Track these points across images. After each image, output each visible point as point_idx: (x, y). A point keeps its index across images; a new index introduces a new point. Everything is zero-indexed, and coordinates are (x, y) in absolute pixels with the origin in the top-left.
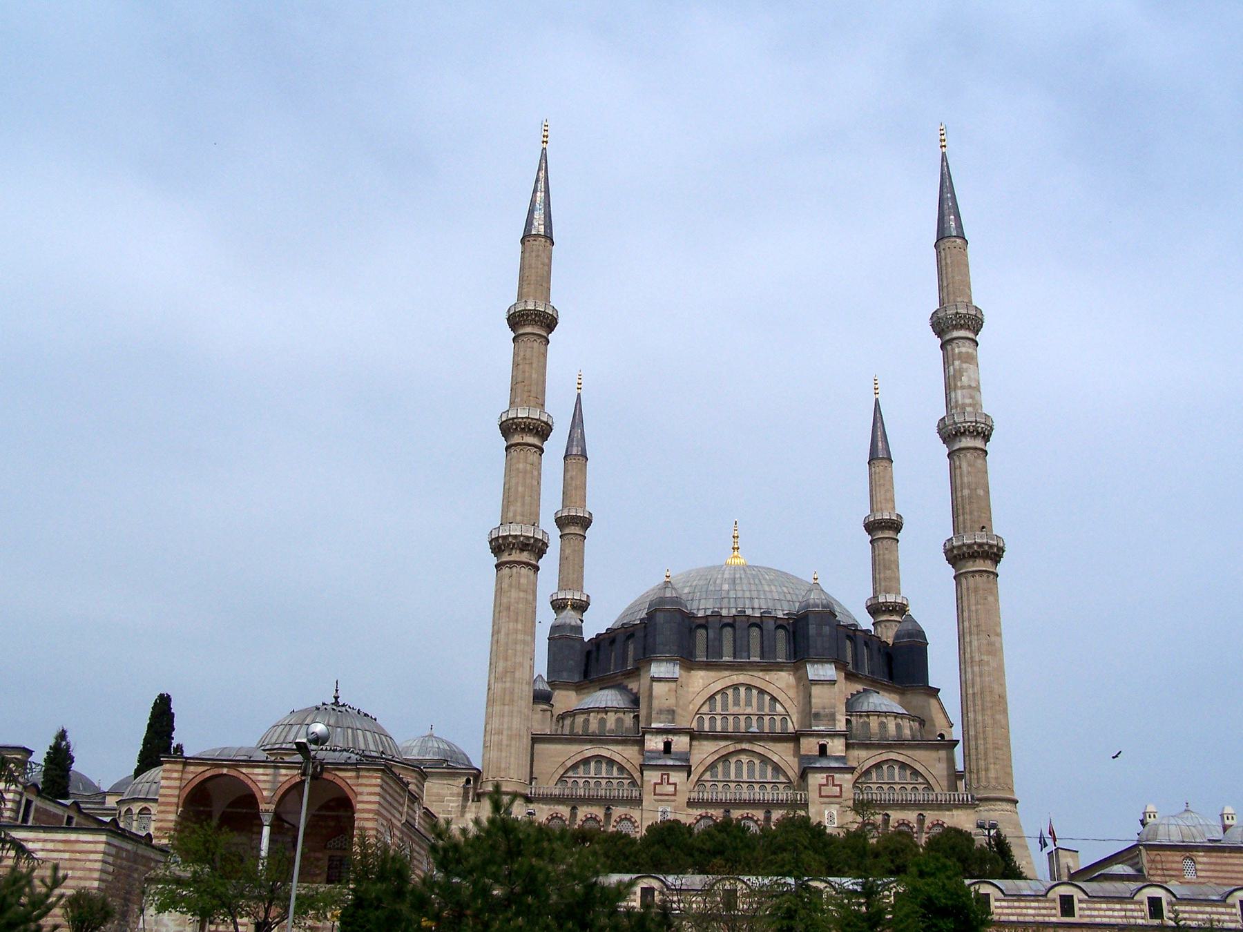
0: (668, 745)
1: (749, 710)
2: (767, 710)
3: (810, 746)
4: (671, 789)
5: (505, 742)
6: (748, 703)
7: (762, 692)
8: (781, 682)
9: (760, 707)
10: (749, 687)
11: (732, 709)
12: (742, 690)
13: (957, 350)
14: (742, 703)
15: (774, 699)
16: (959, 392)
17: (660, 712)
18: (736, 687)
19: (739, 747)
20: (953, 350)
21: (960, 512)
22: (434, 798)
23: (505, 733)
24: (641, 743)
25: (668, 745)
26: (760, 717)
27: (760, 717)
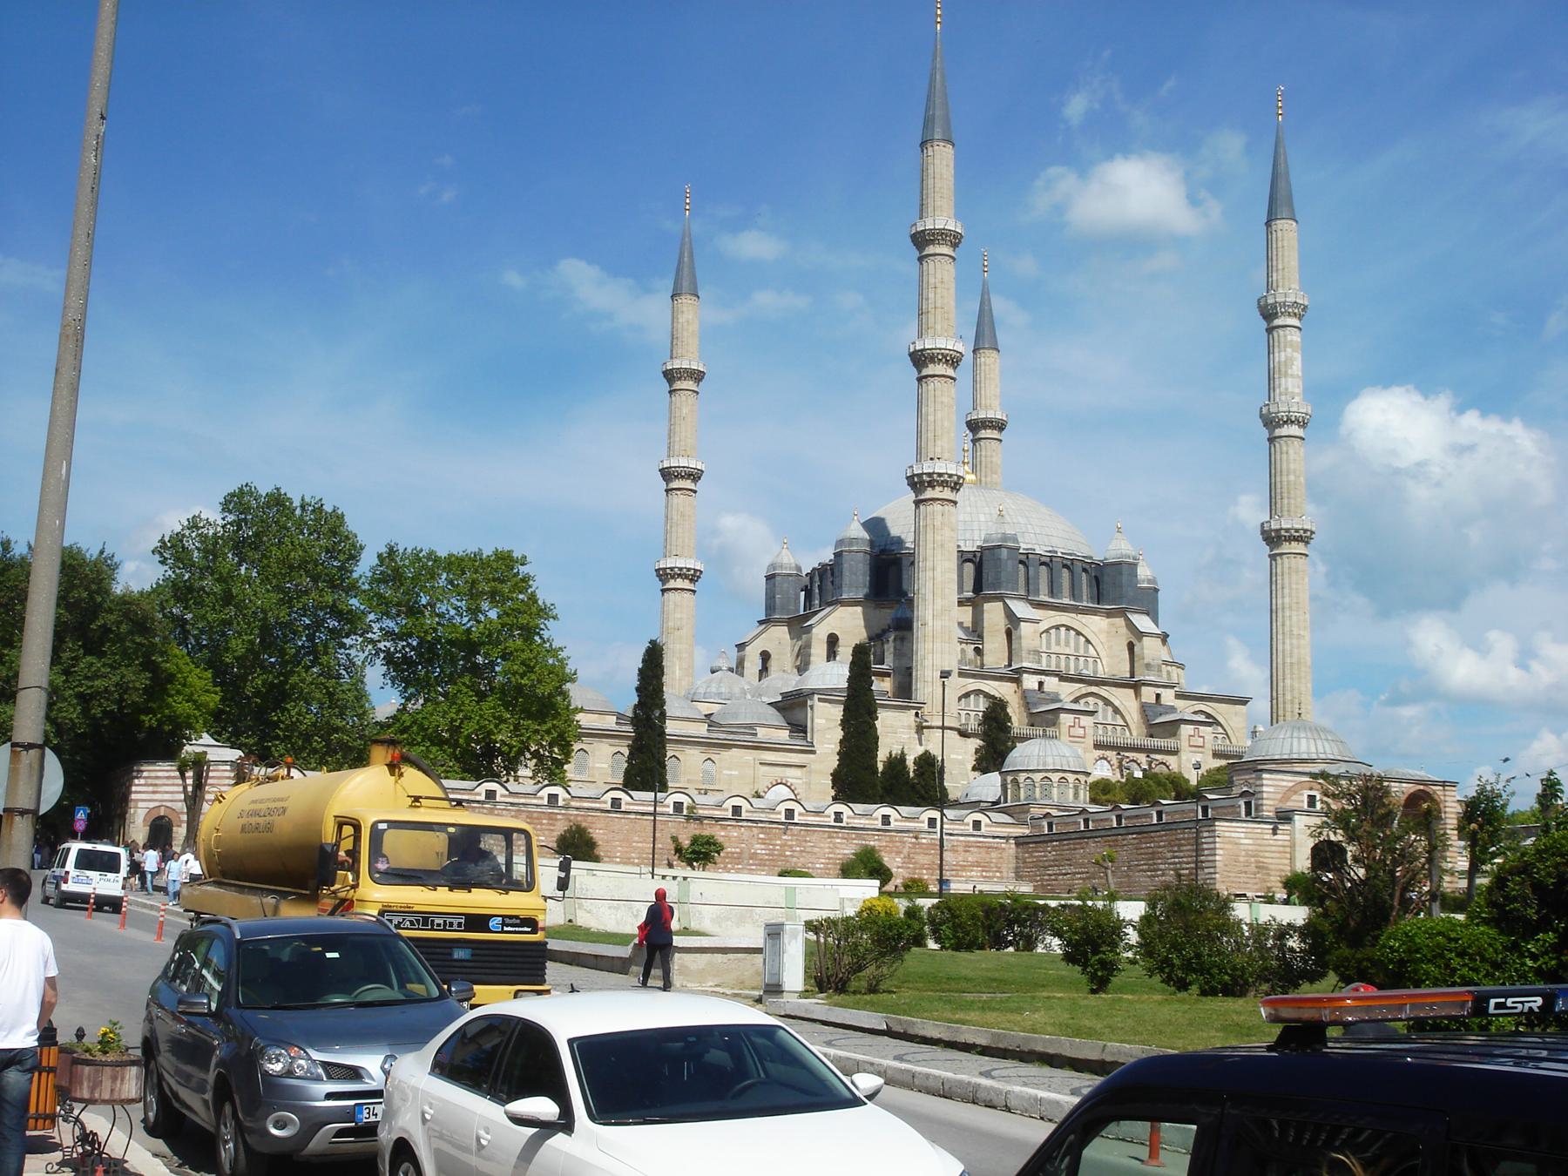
0: (1041, 684)
2: (1082, 652)
3: (1148, 694)
4: (1081, 731)
6: (1067, 644)
7: (1079, 633)
8: (1095, 625)
9: (1077, 649)
10: (1068, 628)
11: (1055, 649)
15: (1088, 641)
17: (1029, 652)
18: (1057, 627)
19: (1094, 689)
24: (1018, 681)
25: (1041, 684)
26: (1077, 658)
27: (1077, 658)
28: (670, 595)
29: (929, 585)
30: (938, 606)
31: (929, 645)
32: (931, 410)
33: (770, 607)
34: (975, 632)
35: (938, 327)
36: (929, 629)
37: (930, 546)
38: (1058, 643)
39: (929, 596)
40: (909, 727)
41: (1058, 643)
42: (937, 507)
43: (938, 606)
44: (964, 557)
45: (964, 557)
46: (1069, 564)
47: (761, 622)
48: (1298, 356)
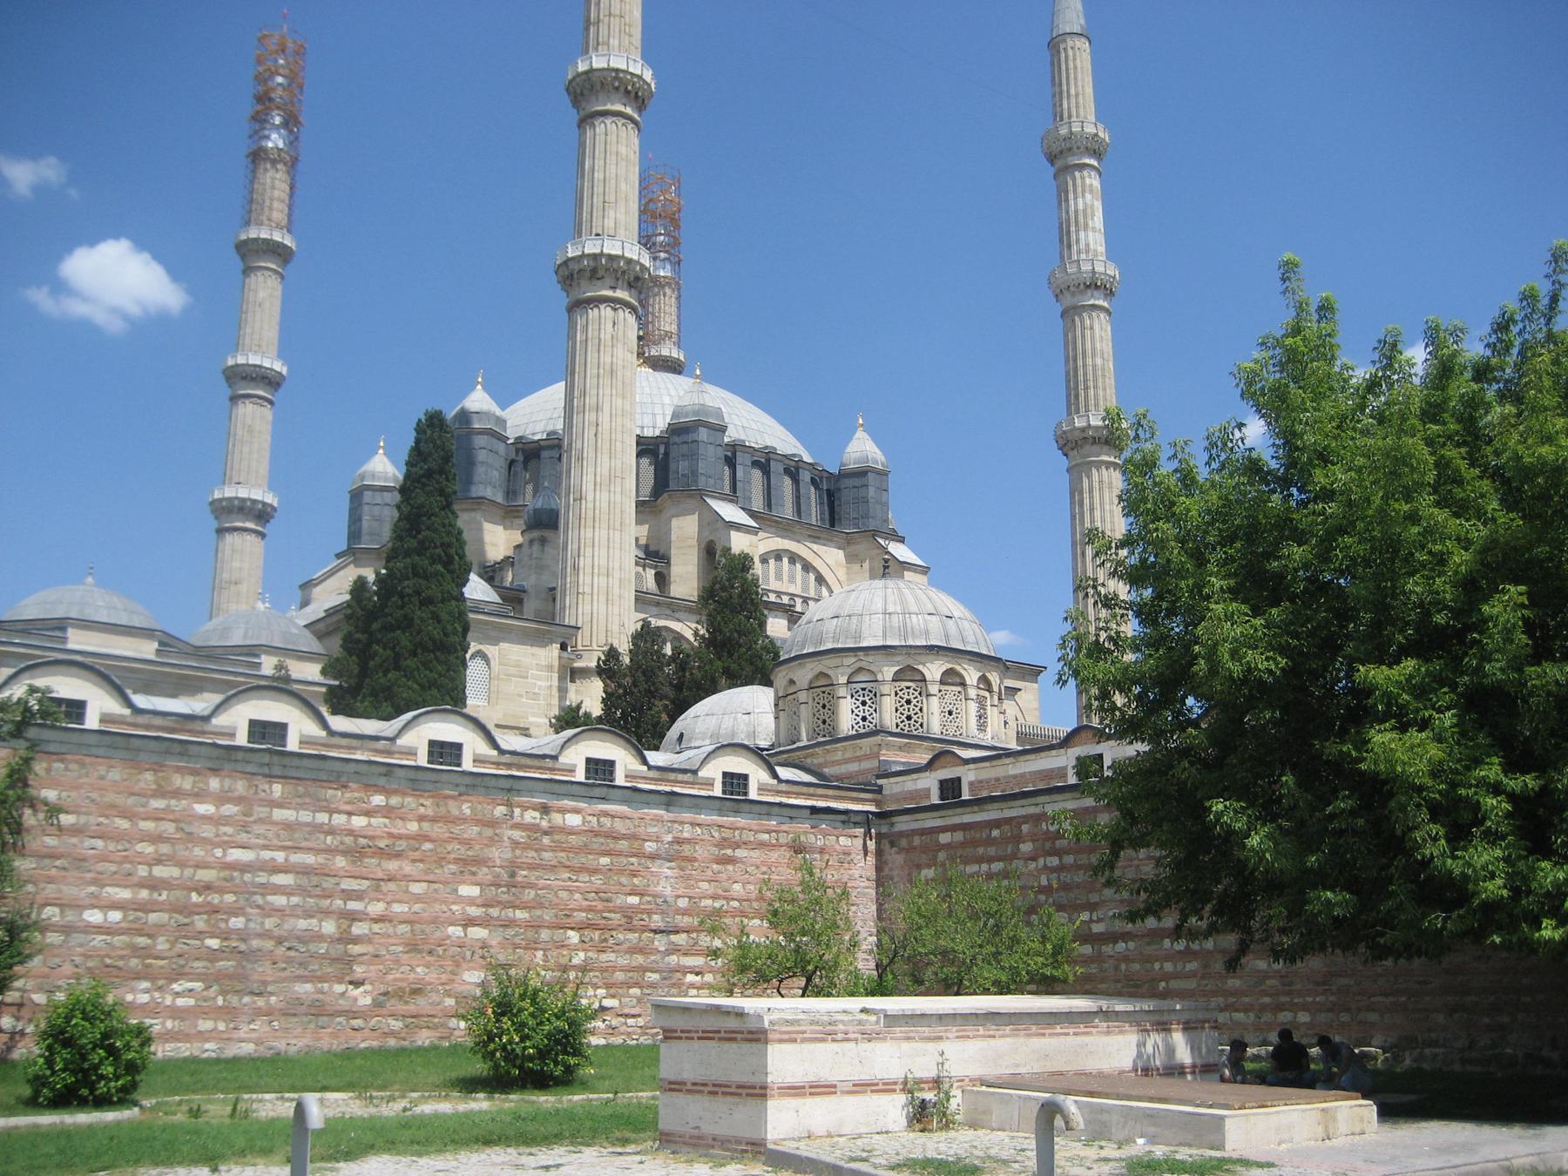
1: (792, 590)
2: (812, 594)
5: (616, 591)
6: (792, 579)
7: (807, 567)
9: (805, 587)
12: (785, 560)
13: (1088, 181)
14: (785, 577)
15: (820, 580)
16: (1090, 233)
20: (1083, 178)
21: (1091, 384)
22: (513, 670)
23: (617, 575)
28: (229, 538)
29: (589, 434)
30: (604, 469)
31: (587, 533)
32: (599, 163)
33: (354, 535)
34: (655, 556)
35: (614, 42)
36: (587, 505)
37: (591, 371)
38: (779, 577)
39: (589, 453)
40: (550, 668)
41: (779, 577)
42: (606, 312)
43: (604, 469)
44: (646, 447)
45: (646, 447)
46: (793, 469)
47: (338, 556)
48: (1098, 205)
